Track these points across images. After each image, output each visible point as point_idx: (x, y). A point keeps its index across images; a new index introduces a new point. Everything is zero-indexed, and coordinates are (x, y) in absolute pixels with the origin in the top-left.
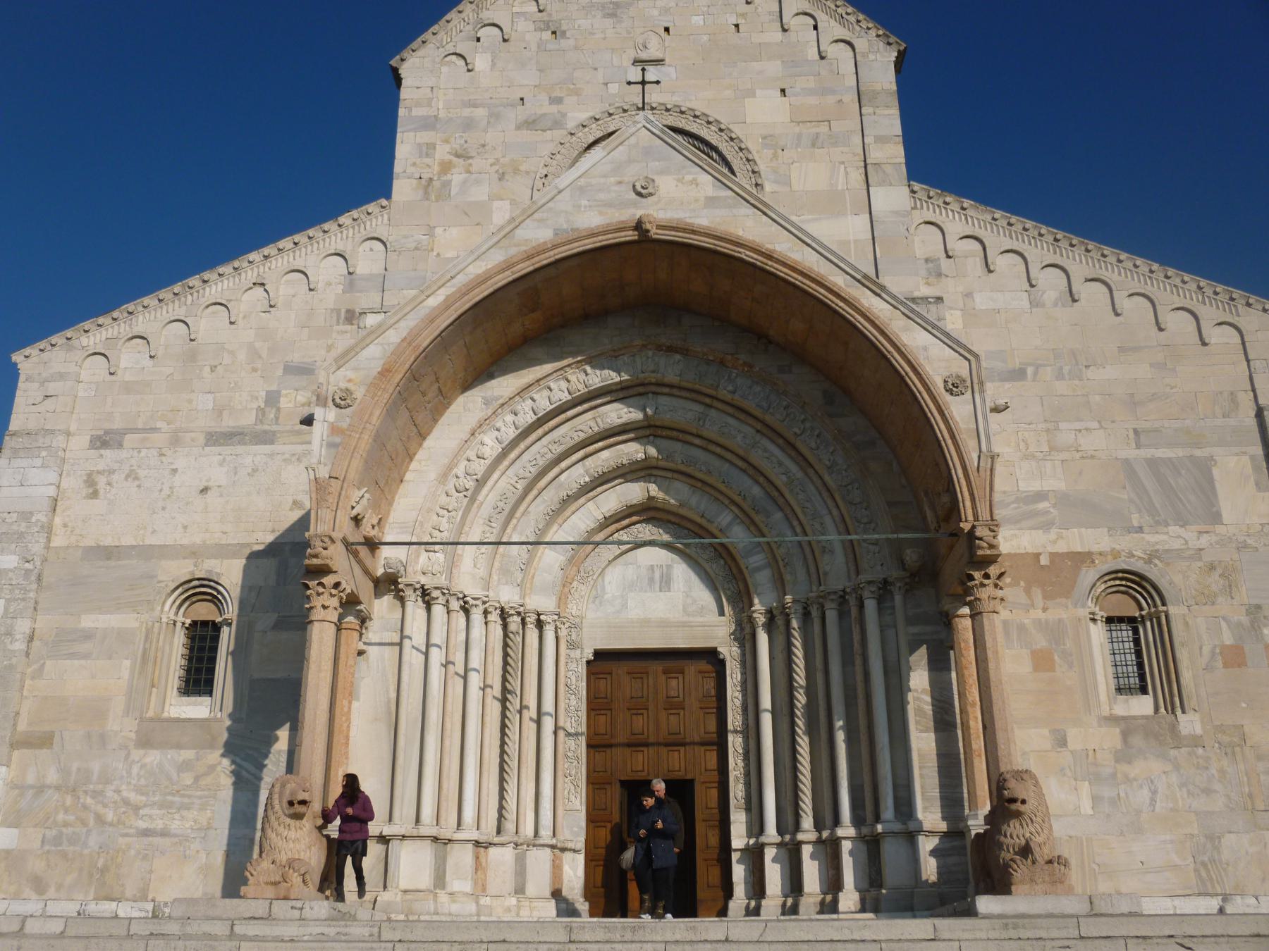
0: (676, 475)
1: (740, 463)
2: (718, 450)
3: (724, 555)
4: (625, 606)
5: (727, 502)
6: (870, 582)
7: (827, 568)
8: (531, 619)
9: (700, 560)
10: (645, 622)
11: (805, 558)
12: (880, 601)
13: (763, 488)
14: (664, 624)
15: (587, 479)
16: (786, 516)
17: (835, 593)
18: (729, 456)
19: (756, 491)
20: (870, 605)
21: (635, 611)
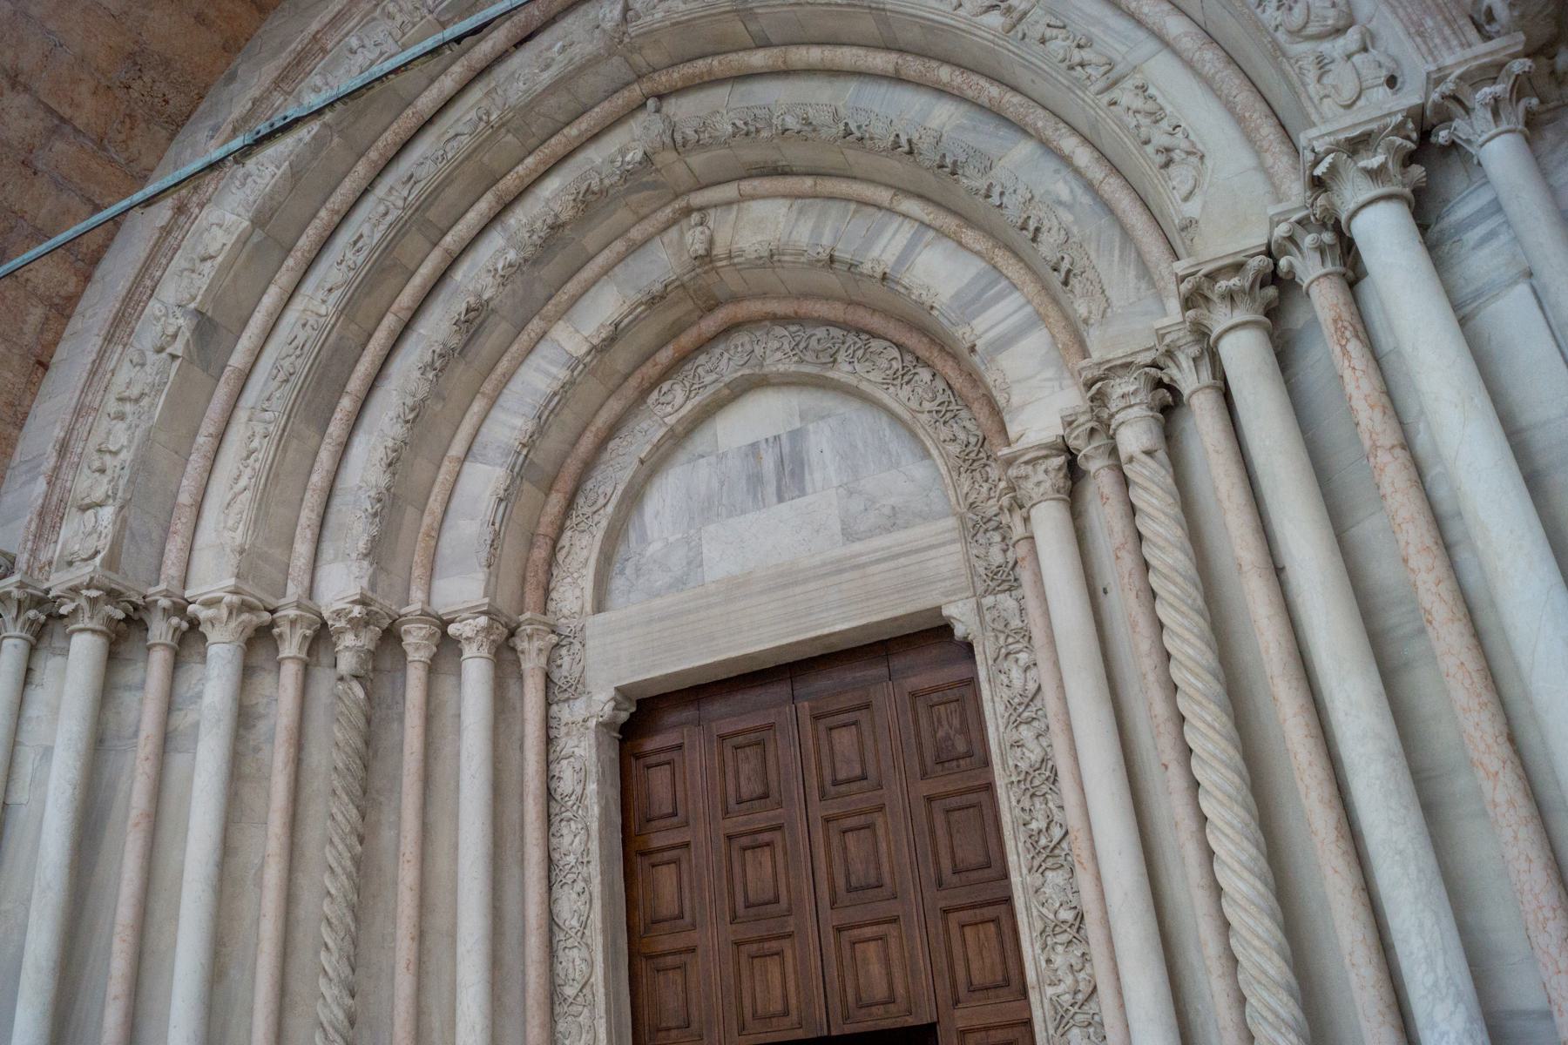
0: (747, 186)
1: (881, 61)
2: (815, 55)
3: (923, 352)
4: (695, 562)
5: (883, 196)
6: (1357, 145)
7: (1192, 209)
8: (417, 640)
9: (864, 386)
10: (737, 587)
11: (1126, 233)
12: (1424, 210)
13: (960, 98)
14: (787, 579)
15: (512, 255)
16: (1046, 146)
17: (1238, 267)
18: (846, 56)
19: (943, 115)
20: (1383, 232)
21: (720, 562)
